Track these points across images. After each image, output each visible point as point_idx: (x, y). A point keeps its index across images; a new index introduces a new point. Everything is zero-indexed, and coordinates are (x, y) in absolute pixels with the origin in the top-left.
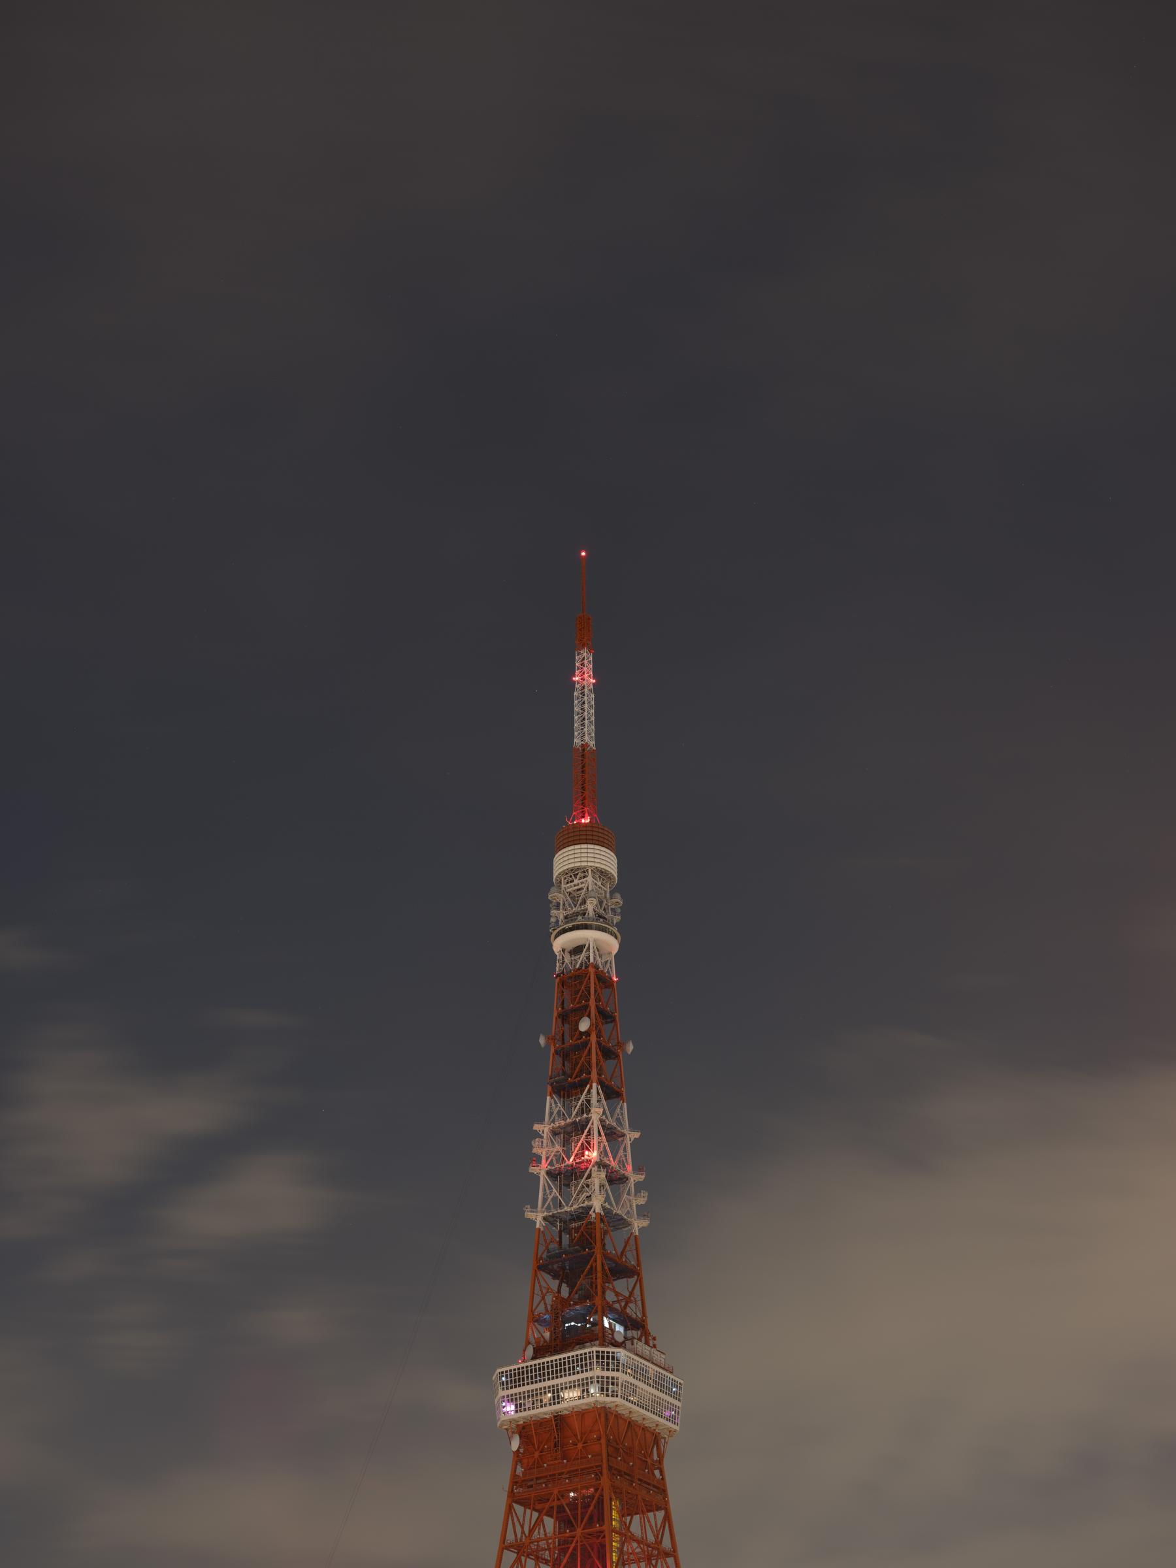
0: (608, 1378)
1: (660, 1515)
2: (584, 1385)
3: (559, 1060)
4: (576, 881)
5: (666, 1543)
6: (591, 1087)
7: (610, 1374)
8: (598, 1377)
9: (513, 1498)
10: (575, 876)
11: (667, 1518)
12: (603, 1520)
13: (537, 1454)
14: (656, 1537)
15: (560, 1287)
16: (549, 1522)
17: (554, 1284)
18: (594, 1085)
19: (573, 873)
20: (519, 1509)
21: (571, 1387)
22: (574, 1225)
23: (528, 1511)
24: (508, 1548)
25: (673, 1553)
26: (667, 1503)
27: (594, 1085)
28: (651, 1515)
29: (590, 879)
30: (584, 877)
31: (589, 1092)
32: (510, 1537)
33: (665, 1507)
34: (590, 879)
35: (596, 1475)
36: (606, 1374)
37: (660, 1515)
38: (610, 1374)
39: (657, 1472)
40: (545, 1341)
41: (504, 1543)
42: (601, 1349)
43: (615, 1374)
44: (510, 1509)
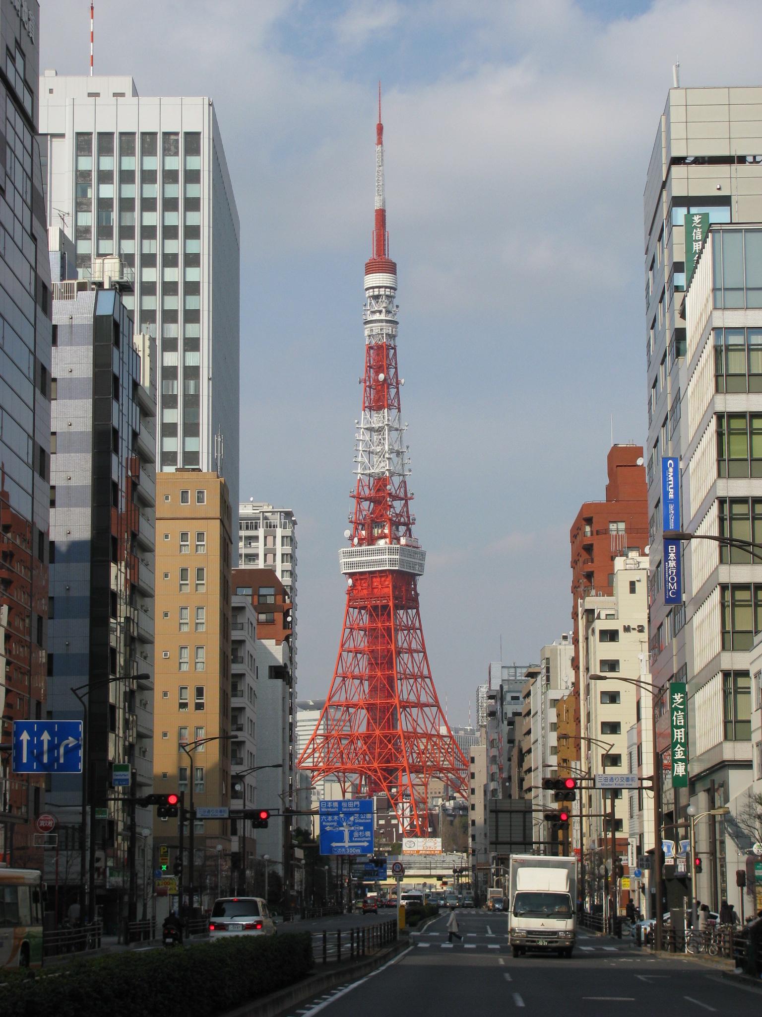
1: (415, 611)
5: (417, 625)
9: (349, 606)
11: (418, 613)
13: (360, 588)
14: (412, 622)
17: (365, 505)
20: (351, 610)
23: (356, 611)
25: (420, 629)
26: (418, 607)
28: (409, 611)
32: (348, 623)
33: (417, 608)
37: (415, 611)
39: (413, 592)
44: (348, 612)
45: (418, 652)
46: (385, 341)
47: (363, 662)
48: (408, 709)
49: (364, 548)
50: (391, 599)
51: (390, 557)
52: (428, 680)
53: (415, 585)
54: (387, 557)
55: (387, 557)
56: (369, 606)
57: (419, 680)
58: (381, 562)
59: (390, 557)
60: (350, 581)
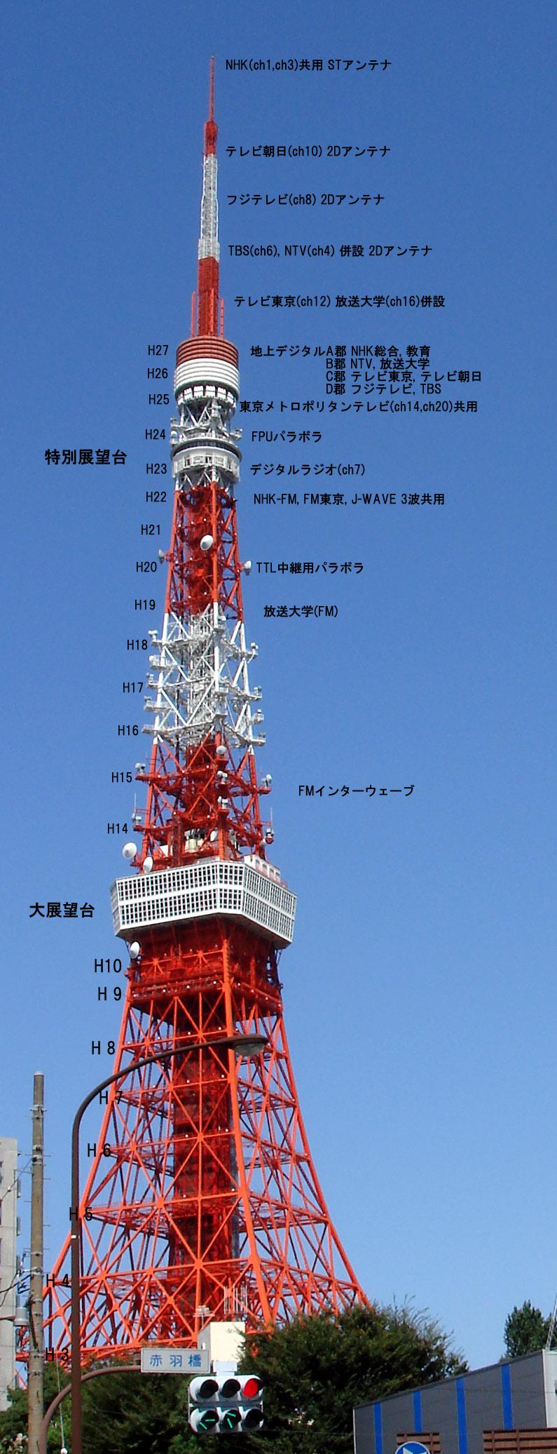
3: (180, 579)
6: (212, 607)
8: (221, 890)
12: (225, 1024)
15: (177, 802)
16: (164, 1026)
18: (216, 604)
20: (136, 1013)
24: (126, 1049)
27: (216, 604)
35: (217, 981)
40: (163, 855)
41: (123, 1044)
43: (238, 887)
45: (288, 1105)
46: (214, 478)
47: (162, 1129)
48: (262, 1235)
49: (169, 871)
50: (226, 979)
51: (223, 886)
52: (304, 1165)
53: (274, 965)
54: (218, 886)
55: (218, 886)
56: (176, 998)
57: (286, 1168)
58: (209, 898)
59: (223, 886)
60: (136, 947)
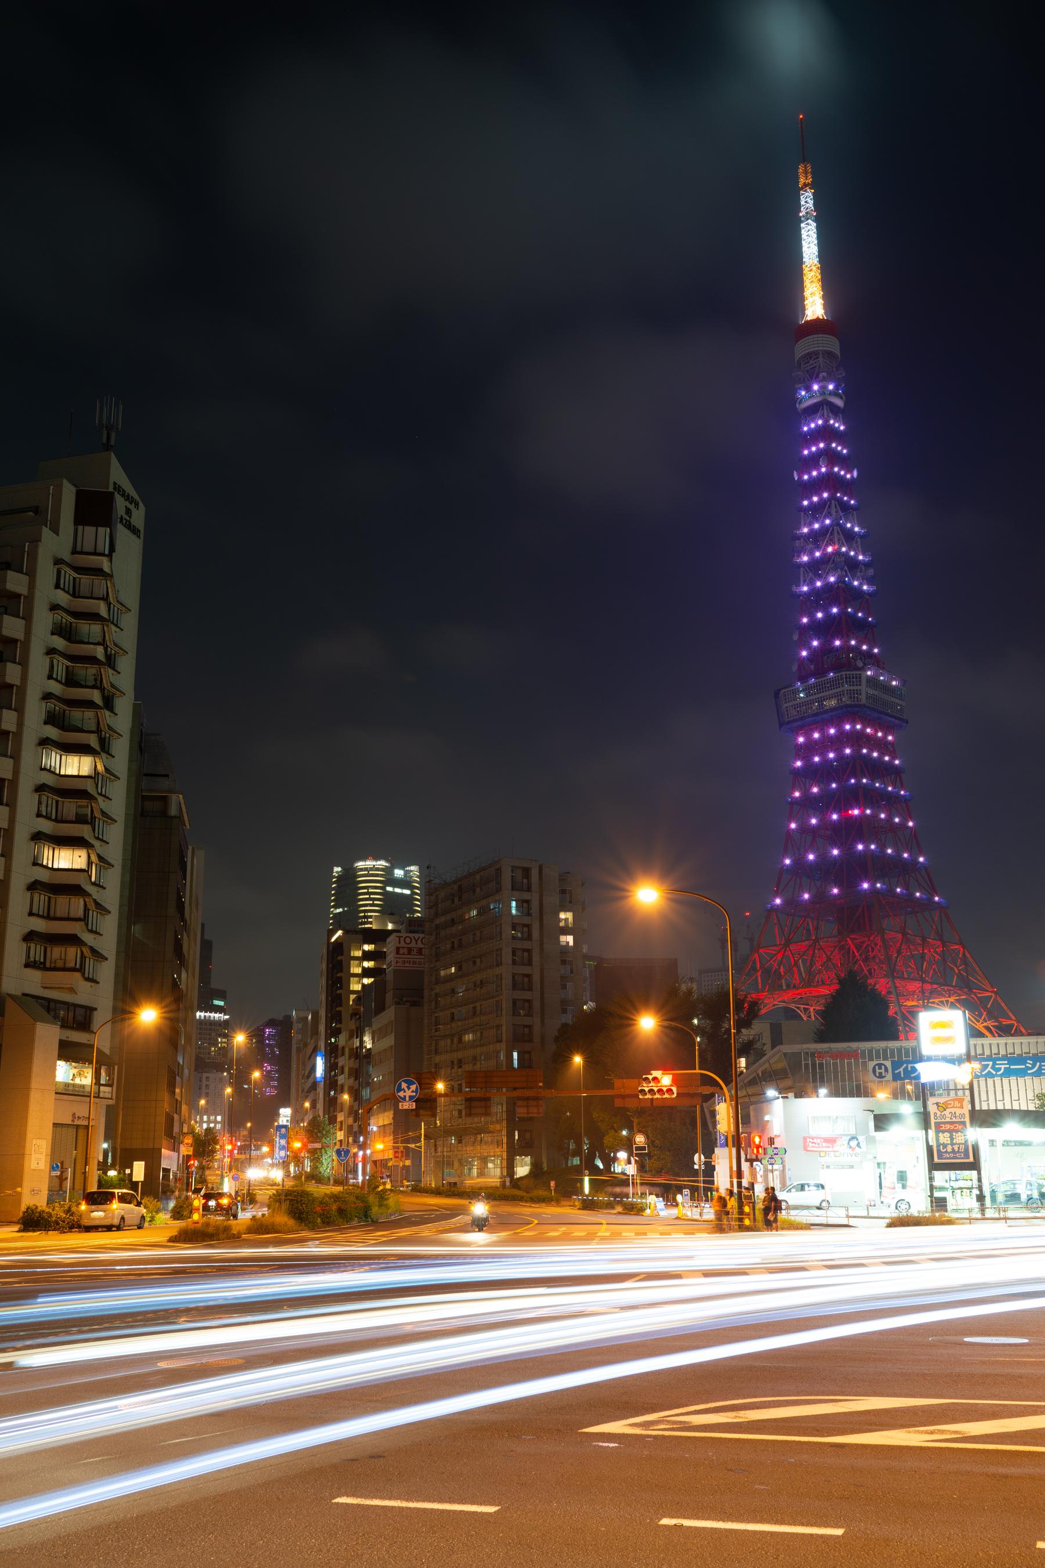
0: (854, 690)
2: (838, 696)
4: (811, 362)
7: (855, 688)
10: (810, 358)
18: (833, 502)
19: (809, 356)
21: (830, 698)
22: (824, 596)
29: (821, 359)
30: (818, 358)
31: (830, 507)
34: (821, 359)
36: (852, 688)
38: (855, 688)
42: (848, 673)
